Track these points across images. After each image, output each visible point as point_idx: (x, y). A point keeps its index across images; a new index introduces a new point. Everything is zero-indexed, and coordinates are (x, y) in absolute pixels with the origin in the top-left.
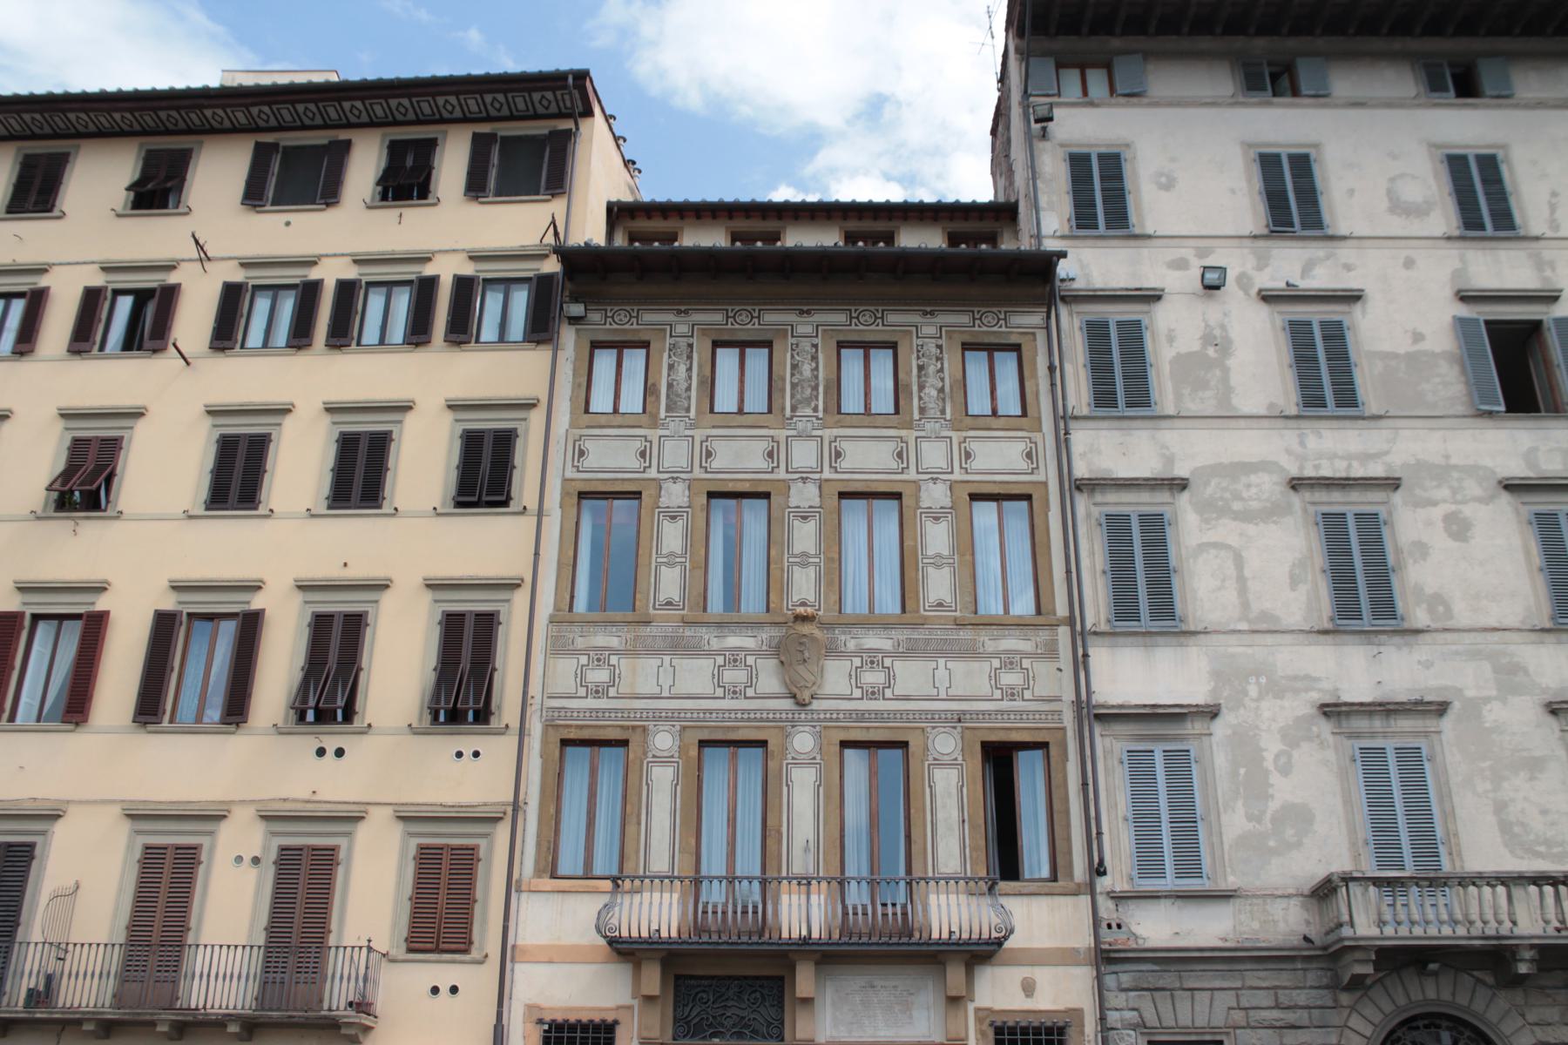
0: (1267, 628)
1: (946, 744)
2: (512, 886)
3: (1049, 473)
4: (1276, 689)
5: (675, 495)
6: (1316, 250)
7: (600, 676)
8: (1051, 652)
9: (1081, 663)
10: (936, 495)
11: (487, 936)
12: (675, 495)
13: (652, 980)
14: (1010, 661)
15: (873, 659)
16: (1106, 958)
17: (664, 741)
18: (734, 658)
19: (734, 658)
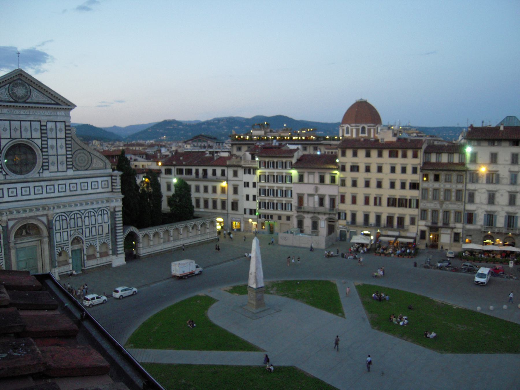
0: (482, 204)
1: (452, 211)
2: (418, 221)
3: (464, 188)
4: (481, 209)
5: (431, 189)
6: (495, 165)
7: (424, 205)
8: (462, 204)
9: (465, 206)
10: (454, 190)
11: (416, 223)
12: (431, 189)
13: (429, 228)
14: (459, 205)
15: (447, 204)
16: (463, 229)
17: (430, 210)
18: (435, 204)
19: (435, 204)
